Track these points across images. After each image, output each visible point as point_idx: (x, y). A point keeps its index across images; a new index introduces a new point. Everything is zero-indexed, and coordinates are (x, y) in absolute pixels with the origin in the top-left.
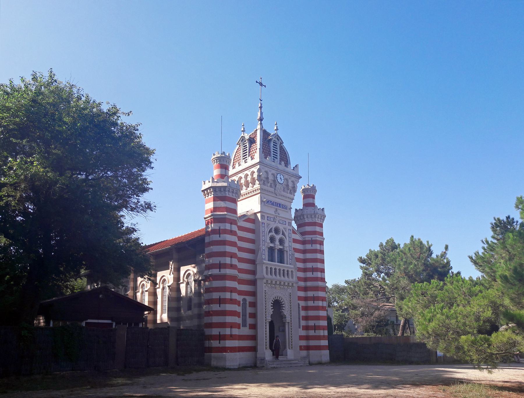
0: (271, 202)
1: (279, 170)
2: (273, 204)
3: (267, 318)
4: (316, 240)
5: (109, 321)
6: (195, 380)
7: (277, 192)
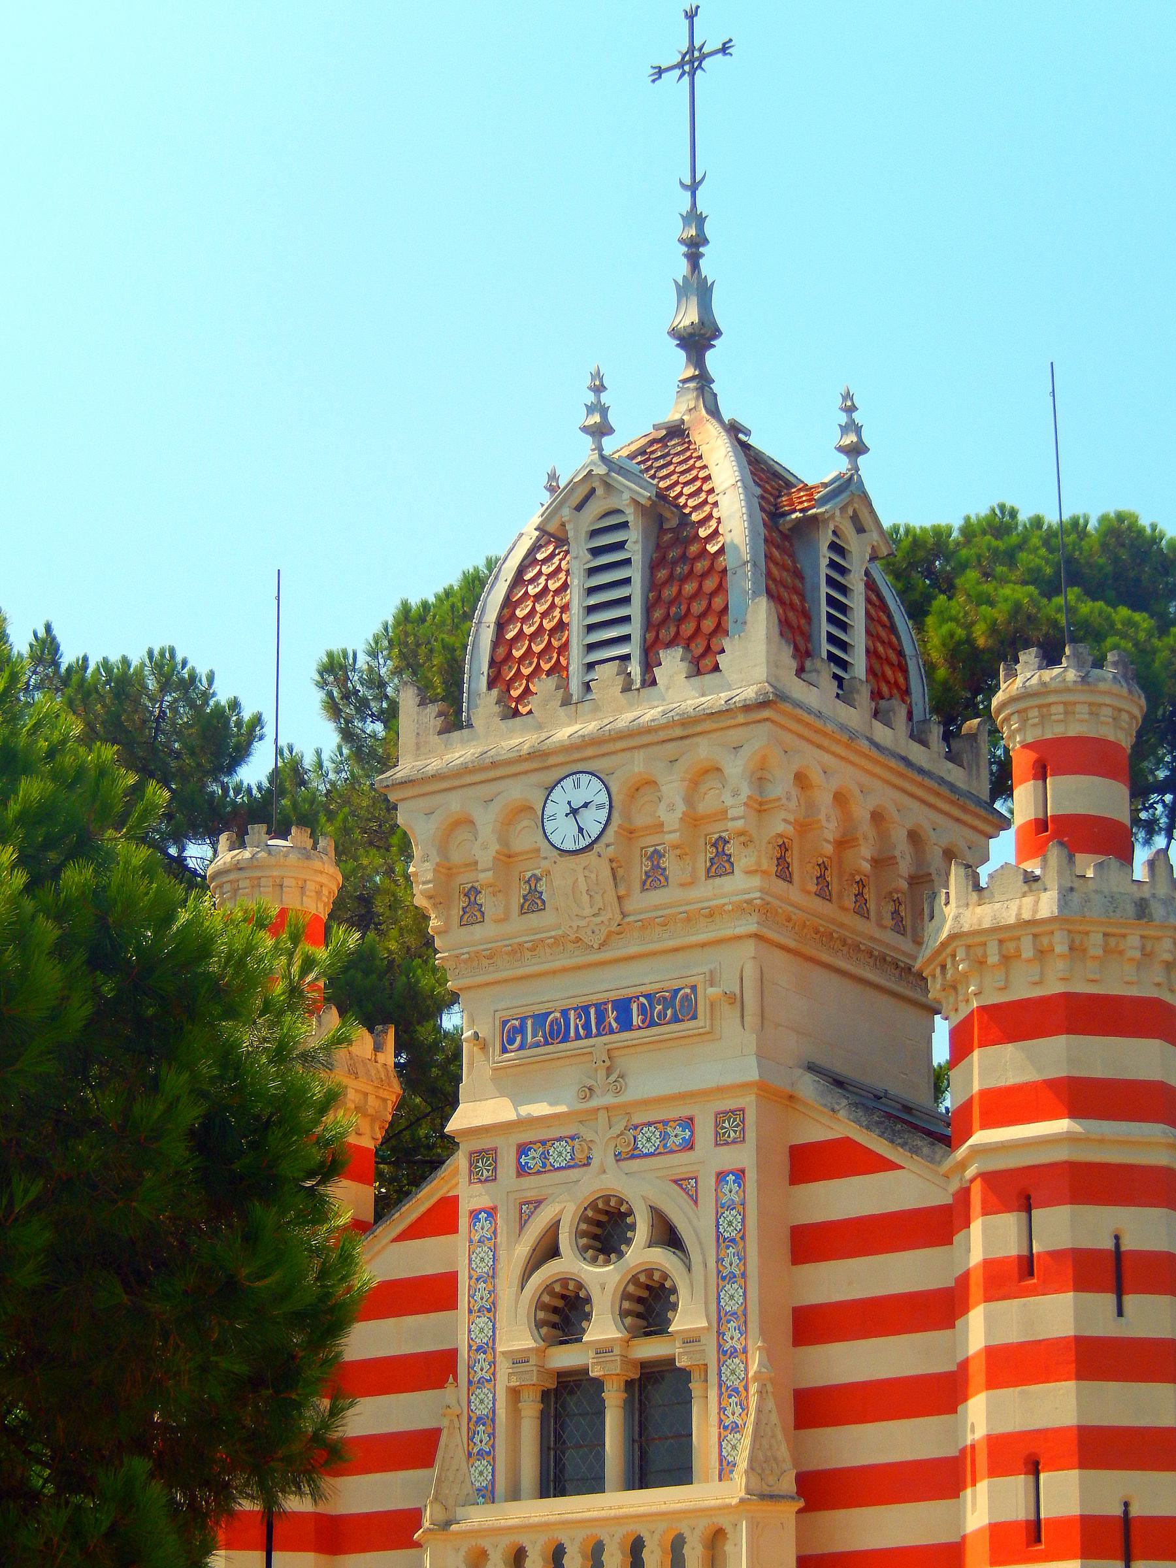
0: (540, 1018)
1: (552, 761)
2: (557, 1033)
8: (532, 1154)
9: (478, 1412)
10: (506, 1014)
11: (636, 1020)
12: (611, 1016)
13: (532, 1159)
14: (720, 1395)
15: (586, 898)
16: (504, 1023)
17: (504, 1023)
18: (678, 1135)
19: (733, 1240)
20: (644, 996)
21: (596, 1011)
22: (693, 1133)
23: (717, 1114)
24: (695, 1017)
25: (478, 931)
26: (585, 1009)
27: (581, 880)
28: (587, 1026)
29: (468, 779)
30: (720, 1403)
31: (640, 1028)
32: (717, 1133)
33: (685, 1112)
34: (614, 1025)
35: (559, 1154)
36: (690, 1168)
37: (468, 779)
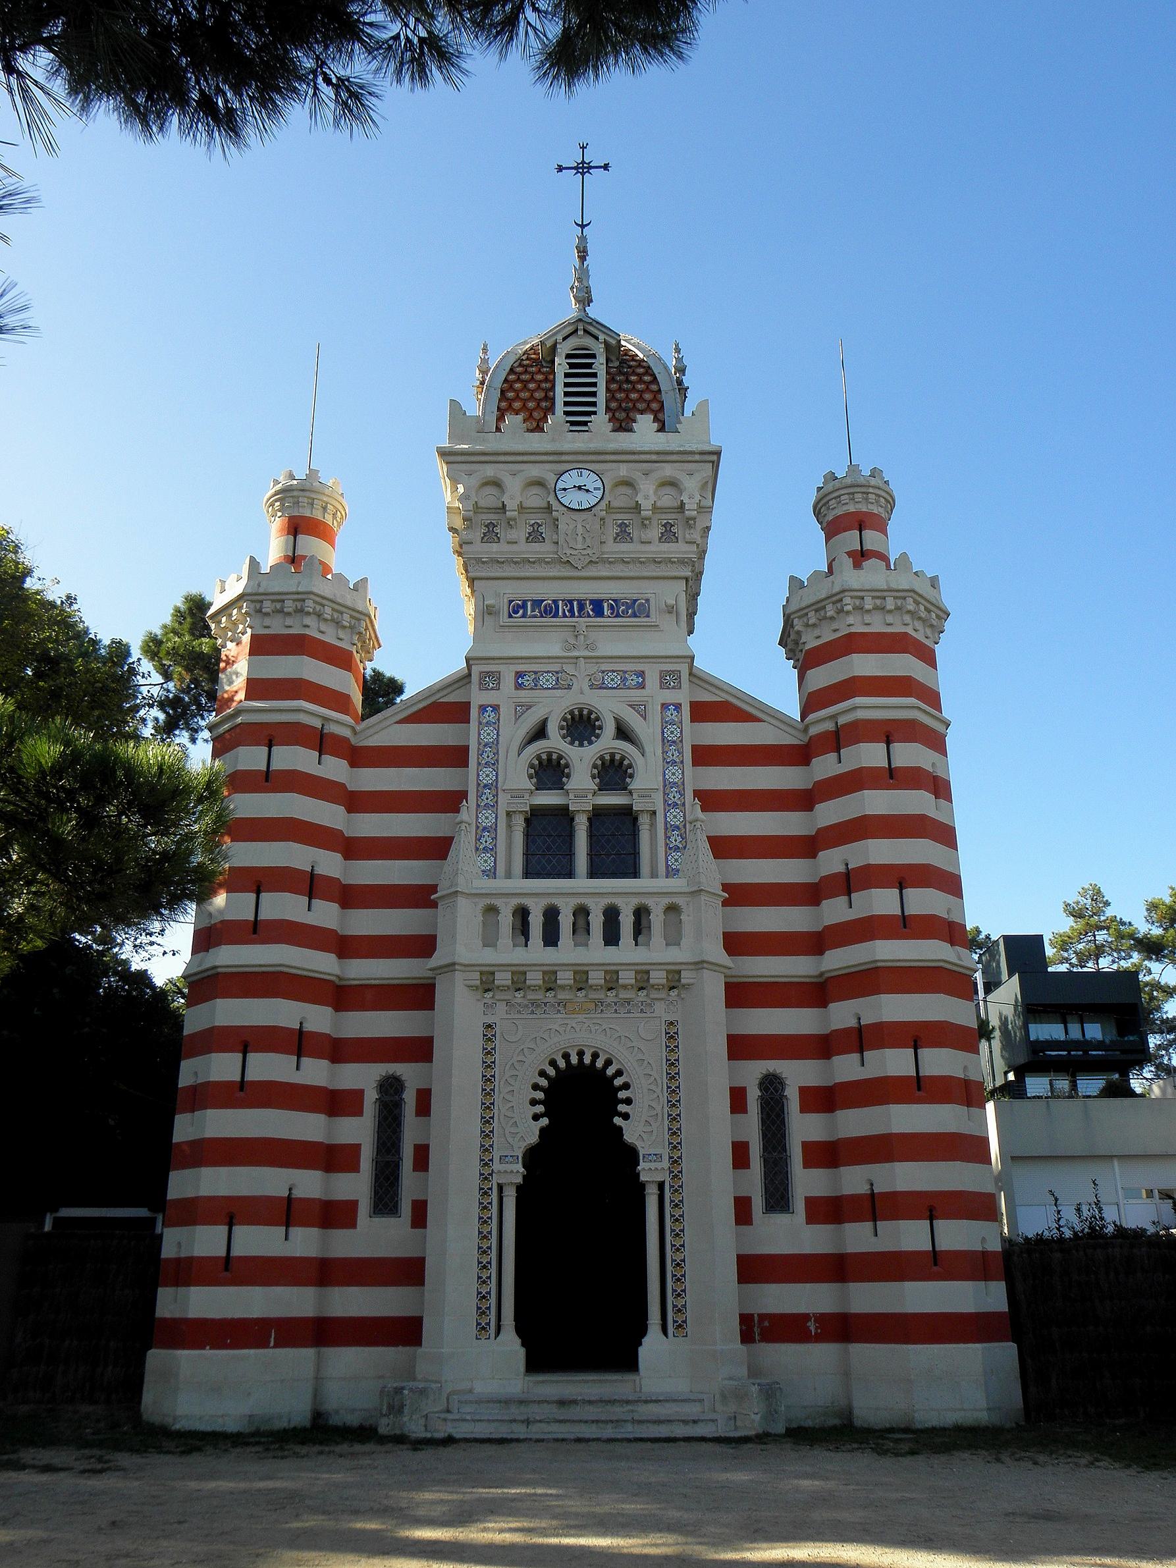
0: (537, 603)
1: (564, 458)
2: (550, 611)
3: (496, 1166)
4: (855, 724)
5: (142, 1212)
6: (518, 1440)
7: (569, 552)
8: (526, 678)
9: (484, 824)
10: (512, 597)
11: (606, 612)
12: (589, 608)
13: (527, 681)
14: (666, 829)
15: (580, 538)
16: (511, 602)
17: (511, 602)
18: (633, 680)
19: (674, 742)
20: (612, 600)
21: (578, 604)
22: (644, 680)
23: (661, 672)
24: (648, 616)
25: (495, 547)
26: (571, 602)
27: (579, 526)
28: (571, 611)
29: (502, 458)
30: (665, 833)
31: (609, 617)
32: (661, 682)
33: (639, 667)
34: (591, 613)
35: (547, 680)
36: (646, 699)
37: (502, 458)
